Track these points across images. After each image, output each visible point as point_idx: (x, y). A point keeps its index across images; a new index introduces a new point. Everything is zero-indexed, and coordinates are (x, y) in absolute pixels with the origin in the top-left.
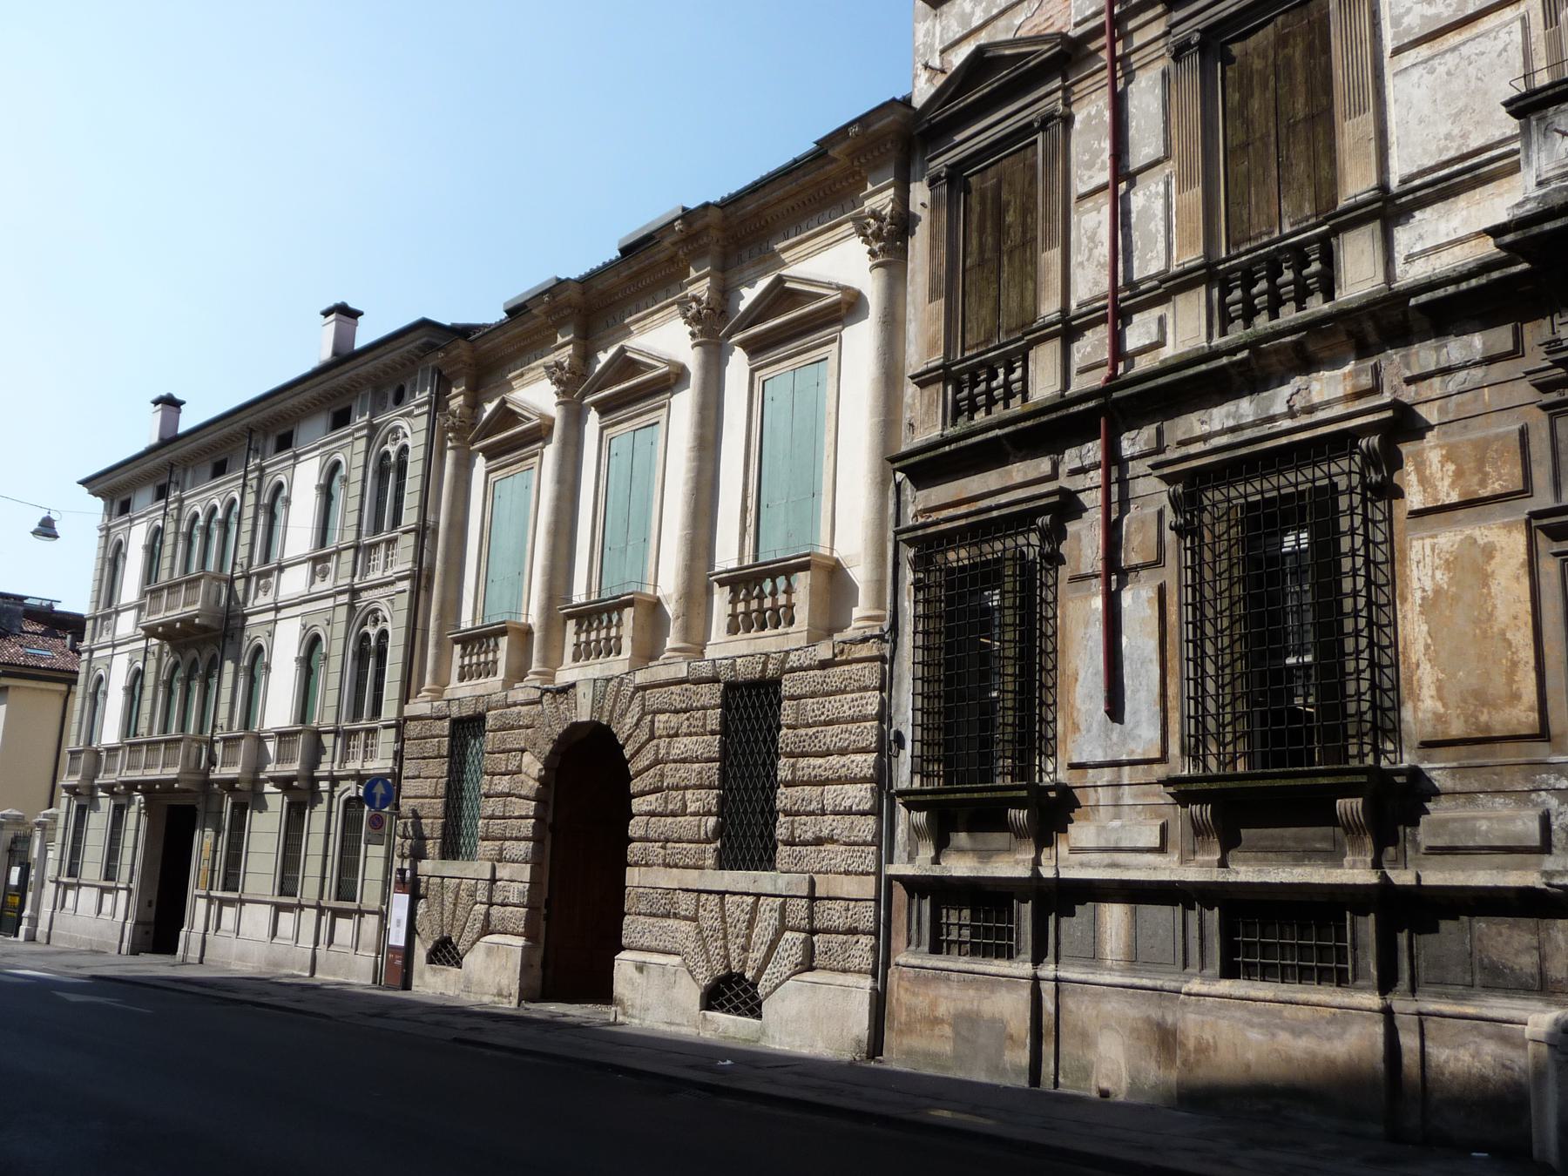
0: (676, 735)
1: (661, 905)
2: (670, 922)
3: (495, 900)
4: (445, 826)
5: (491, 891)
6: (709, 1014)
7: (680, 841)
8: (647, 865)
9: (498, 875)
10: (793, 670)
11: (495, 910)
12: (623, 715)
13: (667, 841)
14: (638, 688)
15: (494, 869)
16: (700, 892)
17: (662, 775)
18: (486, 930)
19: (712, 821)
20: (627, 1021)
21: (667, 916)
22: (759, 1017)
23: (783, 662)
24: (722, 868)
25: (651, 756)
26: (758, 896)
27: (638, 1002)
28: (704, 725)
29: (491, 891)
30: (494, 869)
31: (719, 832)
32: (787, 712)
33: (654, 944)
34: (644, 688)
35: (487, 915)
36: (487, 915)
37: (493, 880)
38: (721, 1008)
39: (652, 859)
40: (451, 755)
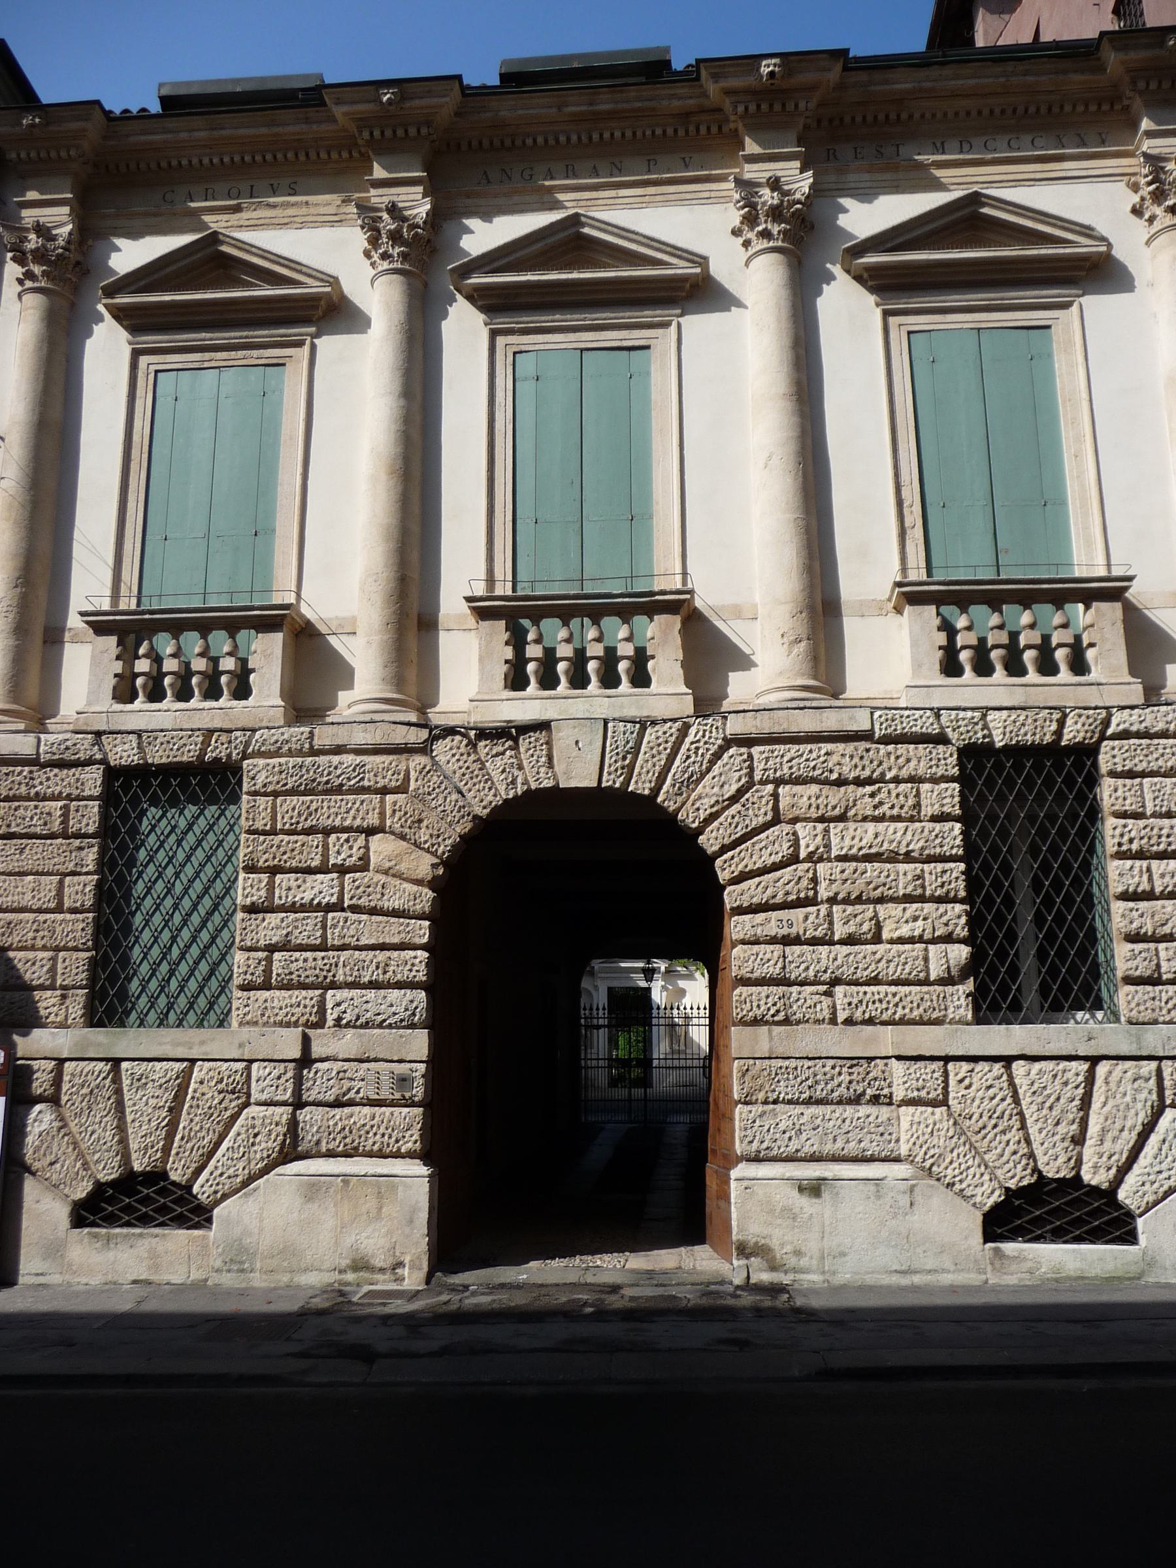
0: (842, 818)
1: (843, 1082)
2: (863, 1110)
3: (309, 1096)
4: (94, 966)
5: (299, 1081)
6: (1009, 1247)
7: (875, 981)
8: (787, 1022)
9: (317, 1050)
10: (1125, 735)
11: (304, 1115)
12: (693, 781)
13: (835, 982)
14: (728, 743)
15: (306, 1041)
16: (947, 1059)
17: (814, 880)
18: (291, 1150)
19: (960, 953)
20: (786, 1279)
21: (856, 1100)
22: (1130, 1237)
23: (1106, 723)
24: (979, 1020)
25: (784, 849)
26: (1094, 1060)
27: (812, 1246)
28: (917, 806)
29: (299, 1081)
30: (306, 1041)
31: (969, 969)
32: (1109, 793)
33: (829, 1148)
34: (748, 742)
35: (293, 1124)
36: (293, 1124)
37: (305, 1061)
38: (1012, 1236)
39: (798, 1013)
40: (106, 831)
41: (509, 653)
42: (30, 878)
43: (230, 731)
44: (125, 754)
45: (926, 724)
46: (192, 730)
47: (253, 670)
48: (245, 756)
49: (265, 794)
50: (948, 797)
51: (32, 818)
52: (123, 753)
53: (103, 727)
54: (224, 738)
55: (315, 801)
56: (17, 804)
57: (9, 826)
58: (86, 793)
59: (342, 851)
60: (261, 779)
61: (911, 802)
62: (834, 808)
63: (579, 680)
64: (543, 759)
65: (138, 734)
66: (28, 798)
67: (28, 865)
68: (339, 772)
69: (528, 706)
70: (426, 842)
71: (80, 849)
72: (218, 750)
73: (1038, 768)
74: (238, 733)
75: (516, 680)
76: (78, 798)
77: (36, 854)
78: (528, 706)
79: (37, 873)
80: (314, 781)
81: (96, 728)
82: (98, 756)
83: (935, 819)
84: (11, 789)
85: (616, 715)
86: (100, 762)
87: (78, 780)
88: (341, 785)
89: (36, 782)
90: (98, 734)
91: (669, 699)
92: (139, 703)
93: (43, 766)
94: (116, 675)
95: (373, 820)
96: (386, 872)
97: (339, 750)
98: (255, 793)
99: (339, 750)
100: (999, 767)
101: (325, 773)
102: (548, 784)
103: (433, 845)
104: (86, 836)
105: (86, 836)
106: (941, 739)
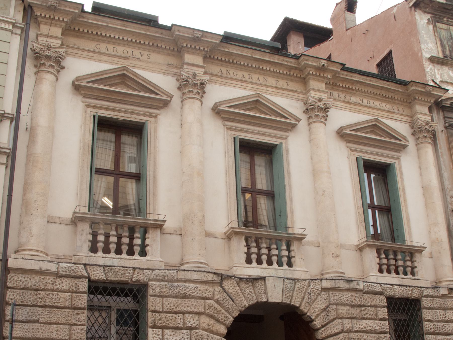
41: (246, 250)
42: (55, 326)
43: (143, 269)
44: (98, 275)
45: (377, 288)
46: (127, 267)
47: (148, 245)
48: (150, 280)
49: (159, 296)
50: (384, 312)
51: (56, 299)
52: (98, 275)
53: (87, 263)
54: (141, 272)
55: (180, 301)
56: (49, 292)
57: (45, 302)
58: (81, 290)
59: (191, 321)
60: (158, 290)
61: (374, 314)
62: (354, 314)
63: (270, 263)
64: (263, 291)
65: (104, 266)
66: (53, 290)
67: (55, 319)
68: (188, 290)
69: (254, 270)
70: (222, 319)
71: (78, 314)
72: (138, 276)
73: (406, 304)
74: (147, 271)
75: (249, 261)
76: (76, 292)
77: (57, 316)
78: (254, 270)
79: (59, 324)
80: (179, 292)
81: (84, 262)
82: (86, 275)
83: (381, 320)
84: (45, 286)
85: (287, 277)
86: (85, 277)
87: (76, 284)
88: (190, 295)
89: (57, 283)
90: (85, 265)
91: (302, 273)
92: (100, 254)
93: (61, 277)
94: (89, 241)
95: (202, 309)
96: (206, 330)
97: (185, 281)
98: (155, 296)
99: (185, 281)
100: (396, 304)
101: (183, 289)
102: (264, 300)
103: (225, 320)
104: (81, 309)
105: (81, 309)
106: (381, 294)
